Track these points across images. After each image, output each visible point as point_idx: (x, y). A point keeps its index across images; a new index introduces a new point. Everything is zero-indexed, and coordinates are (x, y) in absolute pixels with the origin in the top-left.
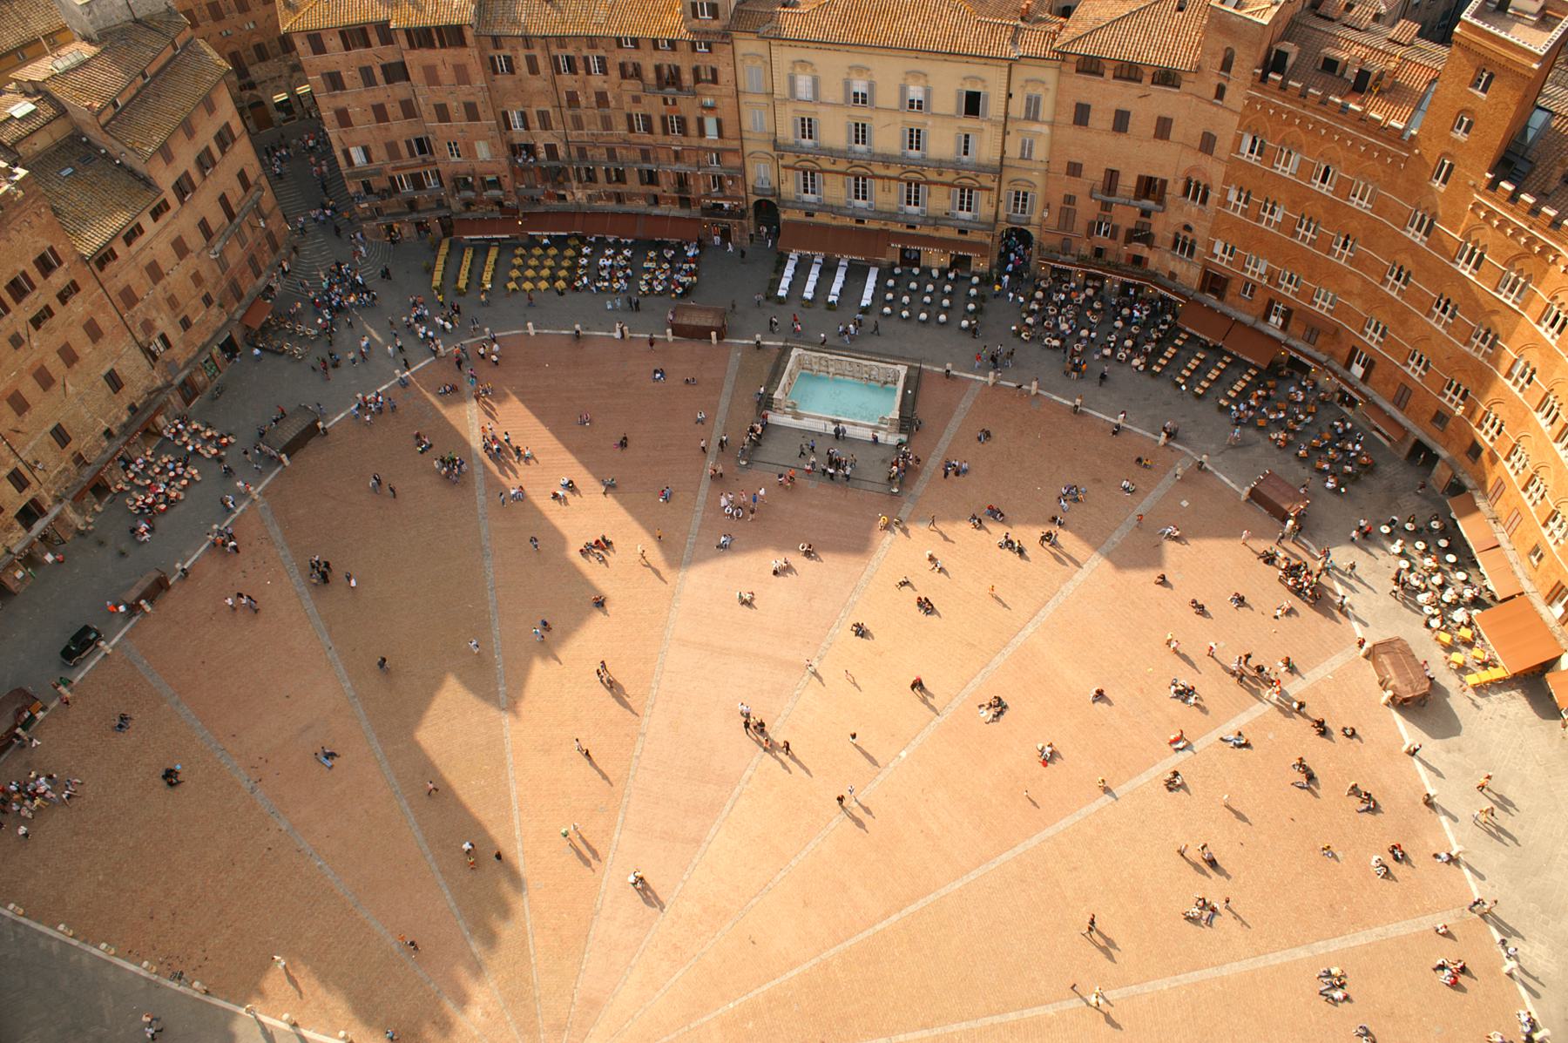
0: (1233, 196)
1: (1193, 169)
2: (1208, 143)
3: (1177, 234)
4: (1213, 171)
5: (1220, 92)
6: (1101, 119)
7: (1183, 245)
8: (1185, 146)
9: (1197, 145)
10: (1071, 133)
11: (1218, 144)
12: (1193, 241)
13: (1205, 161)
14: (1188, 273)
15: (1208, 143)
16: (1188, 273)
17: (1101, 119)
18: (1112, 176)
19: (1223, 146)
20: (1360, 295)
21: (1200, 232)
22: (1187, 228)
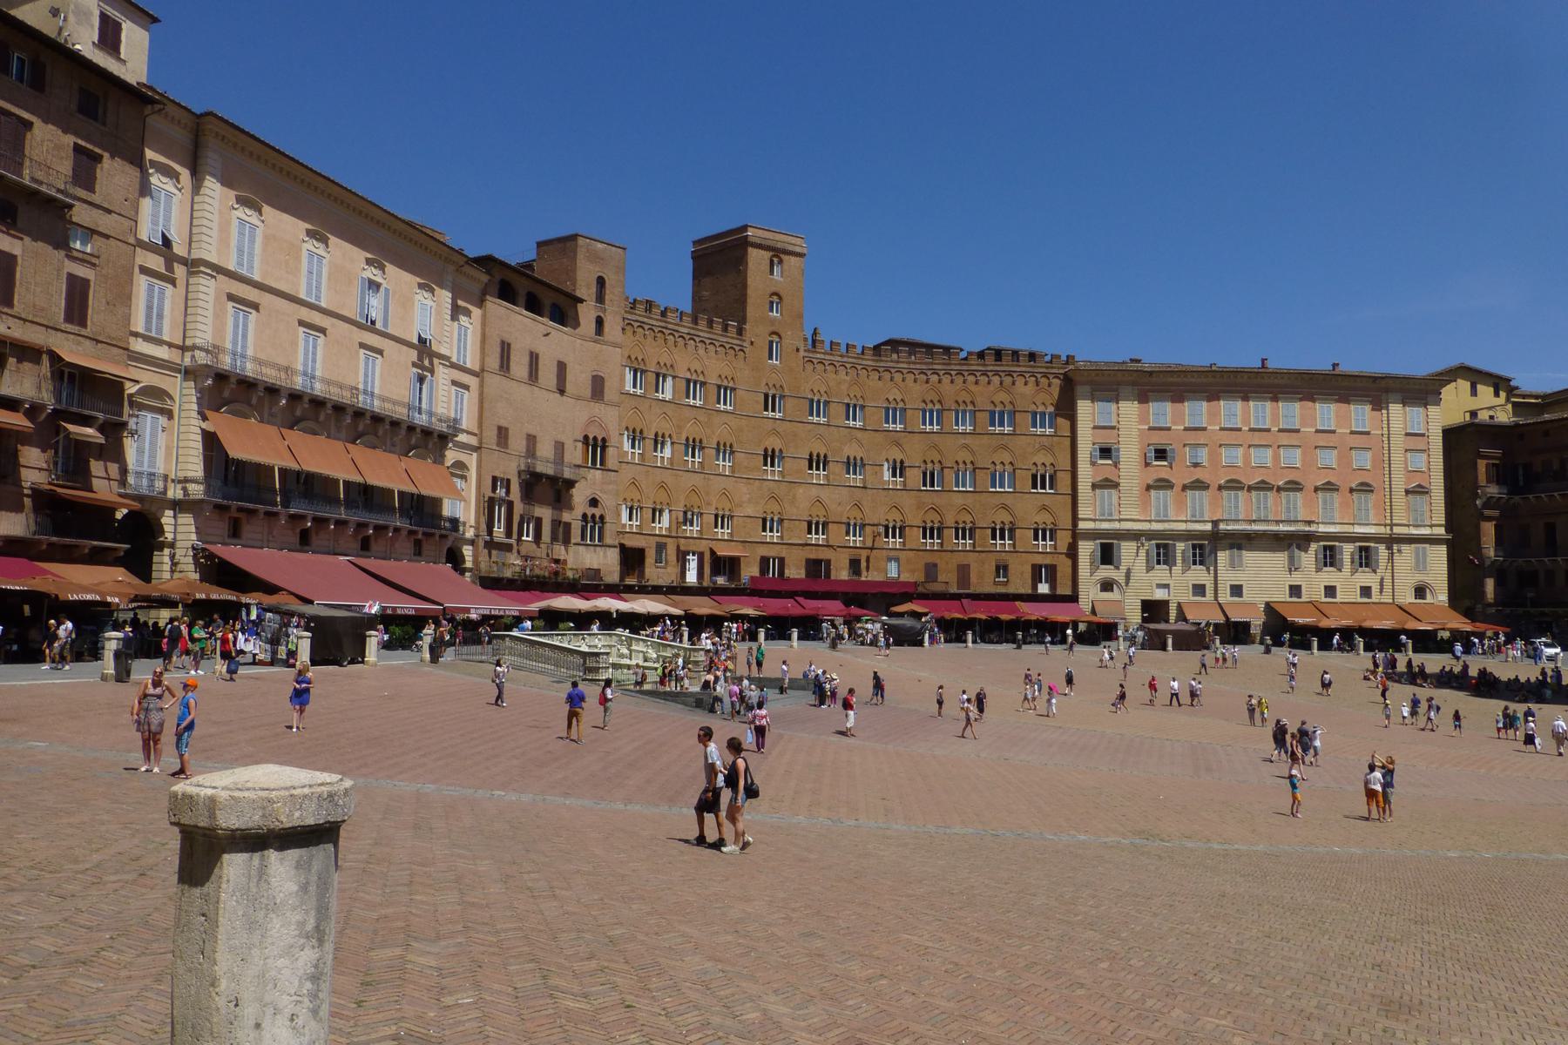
0: (627, 446)
1: (591, 422)
2: (598, 387)
3: (585, 516)
4: (610, 420)
5: (600, 322)
6: (520, 367)
7: (594, 524)
8: (578, 398)
9: (588, 393)
10: (494, 382)
11: (607, 384)
12: (602, 517)
13: (597, 408)
14: (606, 562)
15: (598, 387)
16: (606, 562)
17: (520, 367)
18: (531, 440)
19: (610, 393)
20: (749, 501)
21: (607, 501)
22: (594, 502)
